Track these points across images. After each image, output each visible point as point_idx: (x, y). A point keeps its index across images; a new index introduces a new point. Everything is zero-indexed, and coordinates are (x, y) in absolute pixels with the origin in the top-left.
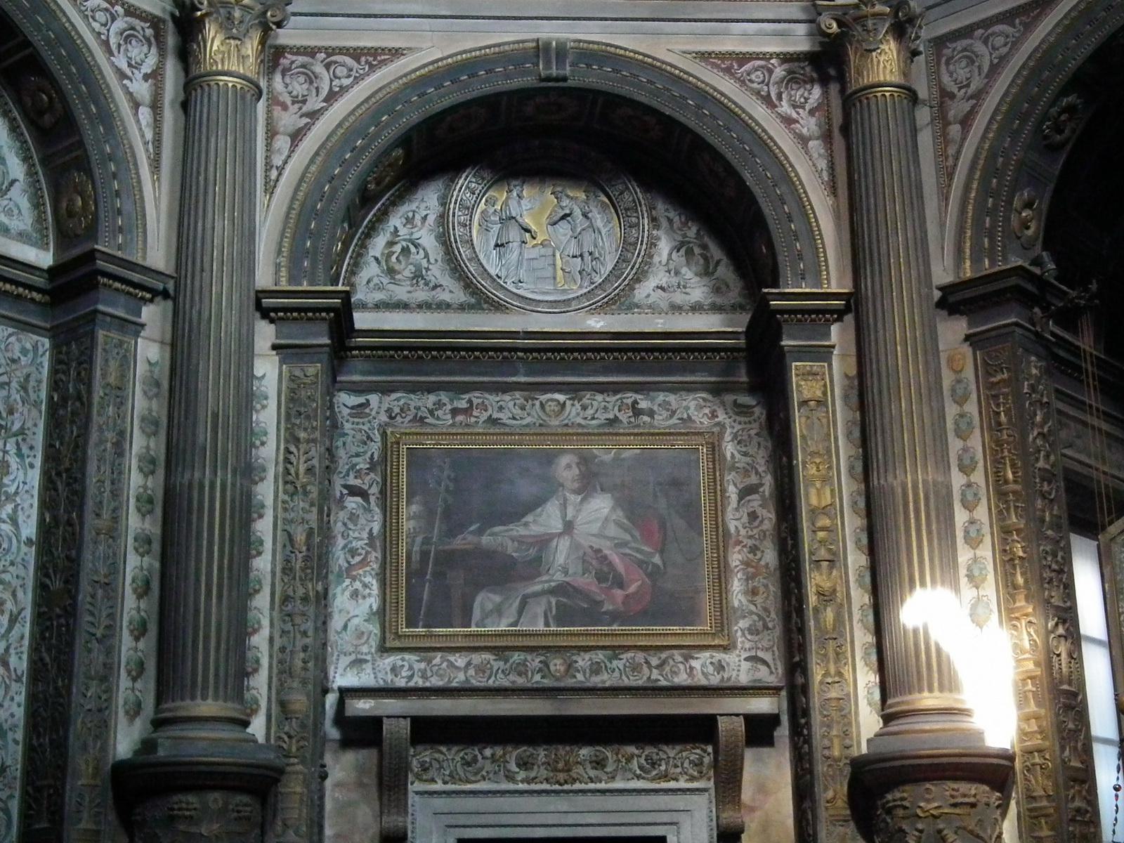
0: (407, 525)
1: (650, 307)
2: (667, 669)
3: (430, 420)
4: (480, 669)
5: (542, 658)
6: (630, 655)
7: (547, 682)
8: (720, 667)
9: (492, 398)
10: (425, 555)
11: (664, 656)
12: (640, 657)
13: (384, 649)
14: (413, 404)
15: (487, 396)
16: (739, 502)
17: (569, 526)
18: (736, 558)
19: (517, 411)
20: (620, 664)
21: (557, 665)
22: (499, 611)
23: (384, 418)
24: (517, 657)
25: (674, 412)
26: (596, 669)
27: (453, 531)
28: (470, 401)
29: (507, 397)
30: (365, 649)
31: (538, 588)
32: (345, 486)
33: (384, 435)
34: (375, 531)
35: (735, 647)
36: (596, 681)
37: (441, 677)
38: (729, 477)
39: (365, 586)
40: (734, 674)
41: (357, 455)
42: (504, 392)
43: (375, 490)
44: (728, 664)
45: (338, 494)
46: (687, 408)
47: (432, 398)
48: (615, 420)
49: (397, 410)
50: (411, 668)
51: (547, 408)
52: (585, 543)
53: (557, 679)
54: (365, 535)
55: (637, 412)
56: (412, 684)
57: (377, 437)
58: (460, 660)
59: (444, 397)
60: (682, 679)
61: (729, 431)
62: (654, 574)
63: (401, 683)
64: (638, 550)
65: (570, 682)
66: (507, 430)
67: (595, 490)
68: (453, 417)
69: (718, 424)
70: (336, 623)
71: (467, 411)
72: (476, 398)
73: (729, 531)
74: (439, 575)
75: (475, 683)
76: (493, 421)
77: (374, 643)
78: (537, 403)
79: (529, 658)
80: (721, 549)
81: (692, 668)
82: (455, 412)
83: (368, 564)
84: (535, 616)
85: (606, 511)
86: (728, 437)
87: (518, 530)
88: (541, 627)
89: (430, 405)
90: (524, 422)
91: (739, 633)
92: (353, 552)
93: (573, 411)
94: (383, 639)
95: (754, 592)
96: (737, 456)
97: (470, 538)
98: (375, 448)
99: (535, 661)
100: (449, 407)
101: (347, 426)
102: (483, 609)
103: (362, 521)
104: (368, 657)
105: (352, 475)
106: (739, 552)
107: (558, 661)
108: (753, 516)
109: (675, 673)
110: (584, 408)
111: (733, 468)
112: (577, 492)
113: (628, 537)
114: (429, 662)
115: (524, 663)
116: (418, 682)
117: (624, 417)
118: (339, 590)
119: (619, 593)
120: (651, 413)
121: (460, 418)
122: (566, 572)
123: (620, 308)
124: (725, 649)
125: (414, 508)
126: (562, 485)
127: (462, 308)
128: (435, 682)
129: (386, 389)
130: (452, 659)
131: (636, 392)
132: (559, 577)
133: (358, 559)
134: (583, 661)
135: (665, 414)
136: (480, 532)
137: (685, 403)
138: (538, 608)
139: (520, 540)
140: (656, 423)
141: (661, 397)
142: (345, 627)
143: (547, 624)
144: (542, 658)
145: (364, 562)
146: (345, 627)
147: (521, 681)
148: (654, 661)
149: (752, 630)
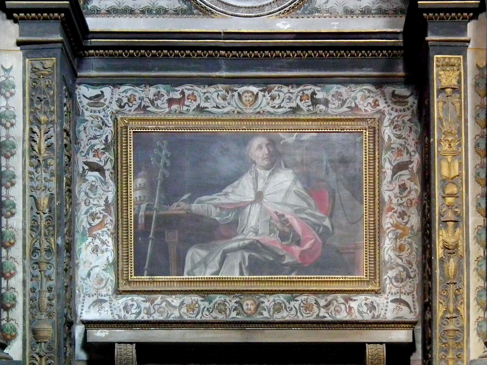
0: (135, 195)
1: (328, 11)
2: (332, 308)
3: (151, 109)
4: (191, 308)
5: (238, 300)
6: (303, 297)
7: (241, 318)
8: (372, 307)
9: (199, 90)
10: (148, 218)
11: (330, 298)
12: (311, 298)
13: (118, 292)
14: (137, 95)
15: (196, 88)
16: (393, 176)
17: (259, 196)
18: (388, 221)
19: (220, 101)
20: (297, 304)
21: (249, 304)
22: (205, 263)
23: (115, 107)
24: (218, 298)
25: (344, 102)
26: (278, 308)
27: (169, 201)
28: (183, 93)
29: (212, 89)
30: (104, 292)
31: (235, 245)
32: (86, 163)
33: (115, 121)
34: (110, 200)
35: (384, 292)
36: (278, 317)
37: (161, 313)
38: (387, 155)
39: (103, 243)
40: (383, 312)
41: (95, 138)
42: (210, 85)
43: (109, 166)
44: (378, 305)
45: (81, 170)
46: (355, 98)
47: (152, 90)
48: (296, 110)
49: (125, 100)
50: (138, 307)
51: (244, 99)
52: (271, 208)
53: (249, 316)
54: (102, 203)
55: (315, 102)
56: (139, 318)
57: (110, 123)
58: (175, 301)
59: (162, 89)
60: (343, 316)
61: (387, 117)
62: (325, 234)
63: (131, 317)
64: (313, 216)
65: (258, 318)
66: (212, 117)
67: (280, 166)
68: (170, 106)
69: (379, 112)
70: (81, 272)
71: (180, 101)
72: (187, 88)
73: (383, 199)
74: (159, 235)
75: (186, 318)
76: (200, 109)
77: (111, 287)
78: (236, 94)
79: (228, 299)
80: (377, 214)
81: (350, 308)
82: (171, 101)
83: (105, 226)
84: (232, 267)
85: (288, 184)
86: (386, 122)
87: (220, 199)
88: (236, 275)
89: (151, 97)
90: (225, 110)
91: (388, 281)
92: (94, 216)
93: (264, 100)
94: (117, 284)
95: (401, 249)
96: (393, 138)
97: (183, 205)
98: (108, 132)
99: (231, 302)
100: (166, 97)
101: (87, 113)
102: (193, 261)
103: (100, 191)
104: (107, 298)
105: (91, 154)
106: (391, 217)
107: (249, 302)
108: (403, 187)
109: (337, 311)
110: (273, 98)
111: (389, 148)
112: (267, 168)
113: (305, 205)
114: (152, 302)
115: (224, 303)
116: (144, 317)
117: (303, 105)
118: (83, 246)
119: (297, 249)
120: (326, 103)
121: (175, 107)
122: (256, 233)
123: (303, 13)
124: (376, 293)
125: (140, 181)
126: (254, 162)
127: (177, 13)
128: (157, 317)
129: (116, 83)
130: (169, 299)
131: (315, 84)
132: (252, 237)
133: (97, 221)
134: (268, 301)
135: (337, 103)
136: (191, 200)
137: (353, 94)
138: (235, 260)
139: (221, 207)
140: (329, 111)
141: (335, 88)
142: (89, 275)
143: (241, 273)
144: (238, 300)
145: (101, 224)
146: (89, 275)
147: (221, 317)
148: (322, 303)
149: (398, 279)
